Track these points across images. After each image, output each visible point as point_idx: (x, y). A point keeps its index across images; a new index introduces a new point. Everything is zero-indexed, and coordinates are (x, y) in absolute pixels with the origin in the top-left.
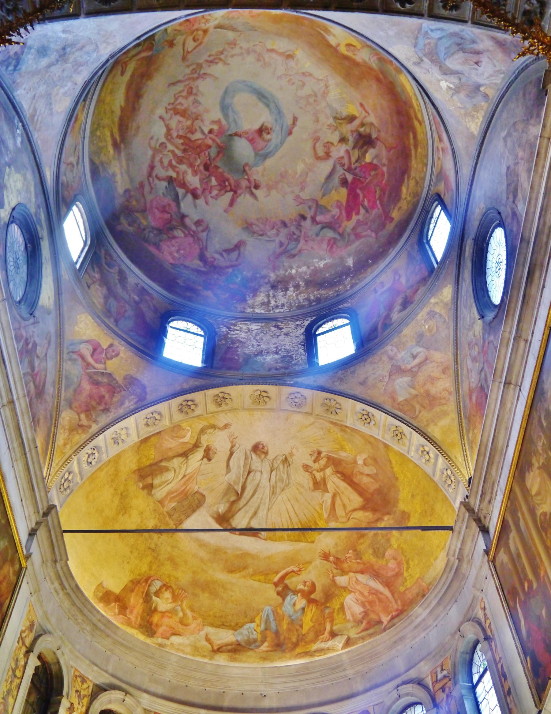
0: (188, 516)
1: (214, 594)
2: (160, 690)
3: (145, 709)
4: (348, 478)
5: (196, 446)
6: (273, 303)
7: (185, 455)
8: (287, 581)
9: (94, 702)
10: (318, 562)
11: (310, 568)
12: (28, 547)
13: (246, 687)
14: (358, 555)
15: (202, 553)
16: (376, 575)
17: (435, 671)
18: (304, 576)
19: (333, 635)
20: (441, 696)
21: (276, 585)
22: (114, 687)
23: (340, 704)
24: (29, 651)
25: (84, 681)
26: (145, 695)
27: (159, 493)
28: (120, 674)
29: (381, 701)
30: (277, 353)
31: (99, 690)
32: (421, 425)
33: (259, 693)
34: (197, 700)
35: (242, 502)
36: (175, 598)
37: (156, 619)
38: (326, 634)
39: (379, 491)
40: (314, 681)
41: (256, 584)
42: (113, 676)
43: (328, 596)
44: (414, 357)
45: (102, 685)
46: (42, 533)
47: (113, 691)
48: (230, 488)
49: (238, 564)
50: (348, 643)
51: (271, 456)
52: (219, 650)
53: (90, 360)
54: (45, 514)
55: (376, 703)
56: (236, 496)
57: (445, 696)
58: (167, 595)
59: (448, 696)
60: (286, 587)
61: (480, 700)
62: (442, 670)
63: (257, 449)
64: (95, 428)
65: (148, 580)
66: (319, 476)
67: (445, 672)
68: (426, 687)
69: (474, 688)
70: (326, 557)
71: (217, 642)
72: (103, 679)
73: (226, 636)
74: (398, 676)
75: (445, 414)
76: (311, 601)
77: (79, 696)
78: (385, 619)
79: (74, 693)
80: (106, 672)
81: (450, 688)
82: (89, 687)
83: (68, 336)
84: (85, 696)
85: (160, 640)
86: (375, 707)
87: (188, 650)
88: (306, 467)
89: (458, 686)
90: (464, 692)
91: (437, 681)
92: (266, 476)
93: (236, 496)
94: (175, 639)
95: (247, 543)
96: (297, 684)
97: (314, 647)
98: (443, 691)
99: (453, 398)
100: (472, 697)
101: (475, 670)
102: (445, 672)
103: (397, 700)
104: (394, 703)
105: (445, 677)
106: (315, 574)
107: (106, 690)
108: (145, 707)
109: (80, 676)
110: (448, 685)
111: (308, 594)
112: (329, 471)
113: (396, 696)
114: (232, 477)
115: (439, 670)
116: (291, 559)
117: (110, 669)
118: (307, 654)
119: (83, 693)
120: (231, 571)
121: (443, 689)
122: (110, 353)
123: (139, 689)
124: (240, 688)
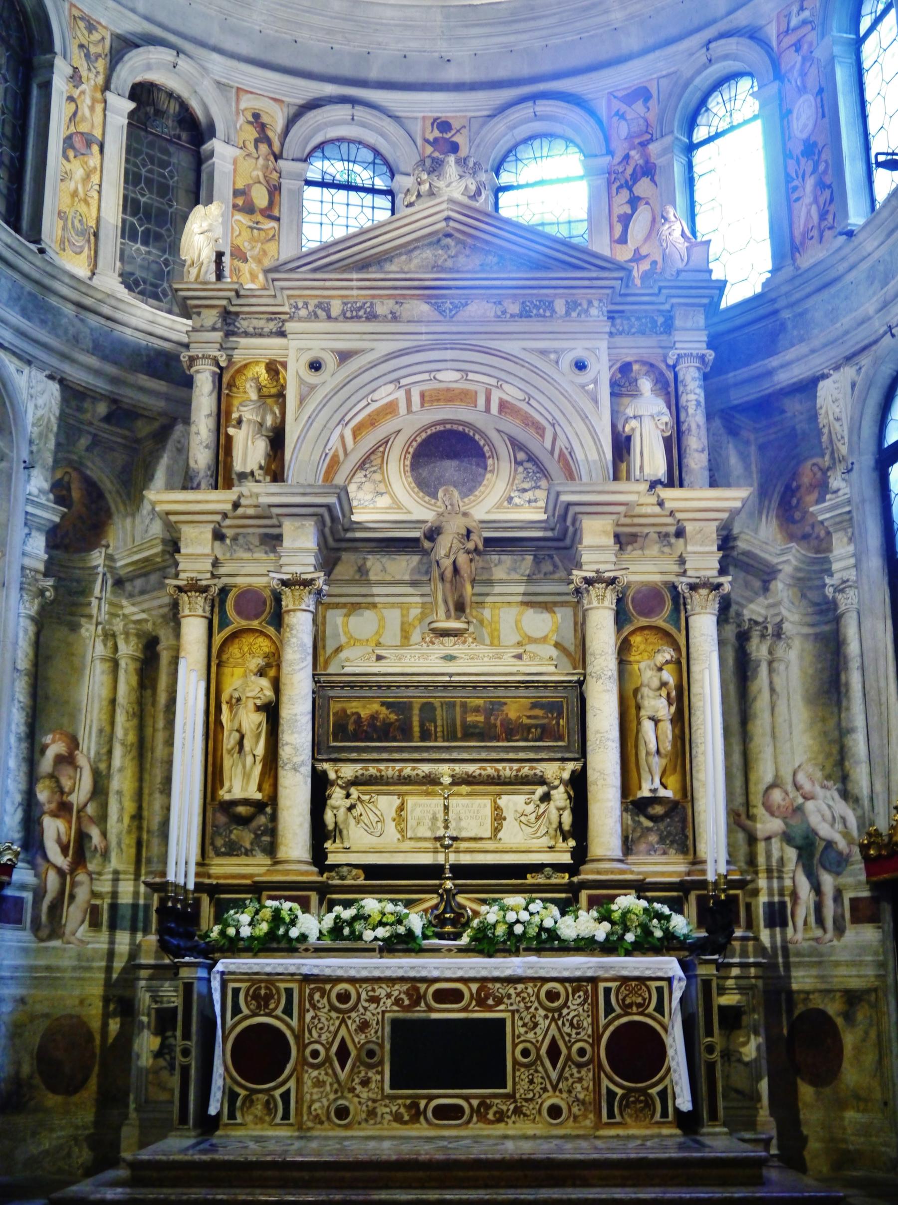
2: (244, 49)
3: (218, 83)
9: (118, 67)
13: (413, 45)
17: (785, 12)
20: (792, 60)
22: (152, 41)
23: (594, 75)
25: (91, 28)
26: (215, 56)
28: (161, 17)
29: (672, 69)
31: (124, 45)
33: (436, 55)
40: (544, 33)
42: (147, 18)
45: (129, 36)
47: (151, 48)
55: (664, 73)
57: (799, 59)
59: (804, 59)
61: (866, 65)
62: (802, 9)
67: (806, 14)
68: (764, 44)
69: (860, 41)
72: (131, 25)
74: (714, 21)
77: (87, 56)
79: (76, 50)
80: (133, 10)
81: (811, 44)
82: (103, 38)
84: (100, 56)
86: (664, 82)
89: (827, 40)
90: (837, 50)
91: (787, 32)
96: (512, 38)
98: (797, 51)
100: (852, 60)
101: (866, 9)
102: (806, 14)
103: (705, 67)
104: (699, 72)
105: (805, 23)
107: (137, 46)
108: (217, 78)
109: (82, 19)
110: (809, 38)
113: (704, 59)
115: (795, 9)
119: (93, 50)
121: (797, 46)
123: (203, 44)
124: (400, 46)
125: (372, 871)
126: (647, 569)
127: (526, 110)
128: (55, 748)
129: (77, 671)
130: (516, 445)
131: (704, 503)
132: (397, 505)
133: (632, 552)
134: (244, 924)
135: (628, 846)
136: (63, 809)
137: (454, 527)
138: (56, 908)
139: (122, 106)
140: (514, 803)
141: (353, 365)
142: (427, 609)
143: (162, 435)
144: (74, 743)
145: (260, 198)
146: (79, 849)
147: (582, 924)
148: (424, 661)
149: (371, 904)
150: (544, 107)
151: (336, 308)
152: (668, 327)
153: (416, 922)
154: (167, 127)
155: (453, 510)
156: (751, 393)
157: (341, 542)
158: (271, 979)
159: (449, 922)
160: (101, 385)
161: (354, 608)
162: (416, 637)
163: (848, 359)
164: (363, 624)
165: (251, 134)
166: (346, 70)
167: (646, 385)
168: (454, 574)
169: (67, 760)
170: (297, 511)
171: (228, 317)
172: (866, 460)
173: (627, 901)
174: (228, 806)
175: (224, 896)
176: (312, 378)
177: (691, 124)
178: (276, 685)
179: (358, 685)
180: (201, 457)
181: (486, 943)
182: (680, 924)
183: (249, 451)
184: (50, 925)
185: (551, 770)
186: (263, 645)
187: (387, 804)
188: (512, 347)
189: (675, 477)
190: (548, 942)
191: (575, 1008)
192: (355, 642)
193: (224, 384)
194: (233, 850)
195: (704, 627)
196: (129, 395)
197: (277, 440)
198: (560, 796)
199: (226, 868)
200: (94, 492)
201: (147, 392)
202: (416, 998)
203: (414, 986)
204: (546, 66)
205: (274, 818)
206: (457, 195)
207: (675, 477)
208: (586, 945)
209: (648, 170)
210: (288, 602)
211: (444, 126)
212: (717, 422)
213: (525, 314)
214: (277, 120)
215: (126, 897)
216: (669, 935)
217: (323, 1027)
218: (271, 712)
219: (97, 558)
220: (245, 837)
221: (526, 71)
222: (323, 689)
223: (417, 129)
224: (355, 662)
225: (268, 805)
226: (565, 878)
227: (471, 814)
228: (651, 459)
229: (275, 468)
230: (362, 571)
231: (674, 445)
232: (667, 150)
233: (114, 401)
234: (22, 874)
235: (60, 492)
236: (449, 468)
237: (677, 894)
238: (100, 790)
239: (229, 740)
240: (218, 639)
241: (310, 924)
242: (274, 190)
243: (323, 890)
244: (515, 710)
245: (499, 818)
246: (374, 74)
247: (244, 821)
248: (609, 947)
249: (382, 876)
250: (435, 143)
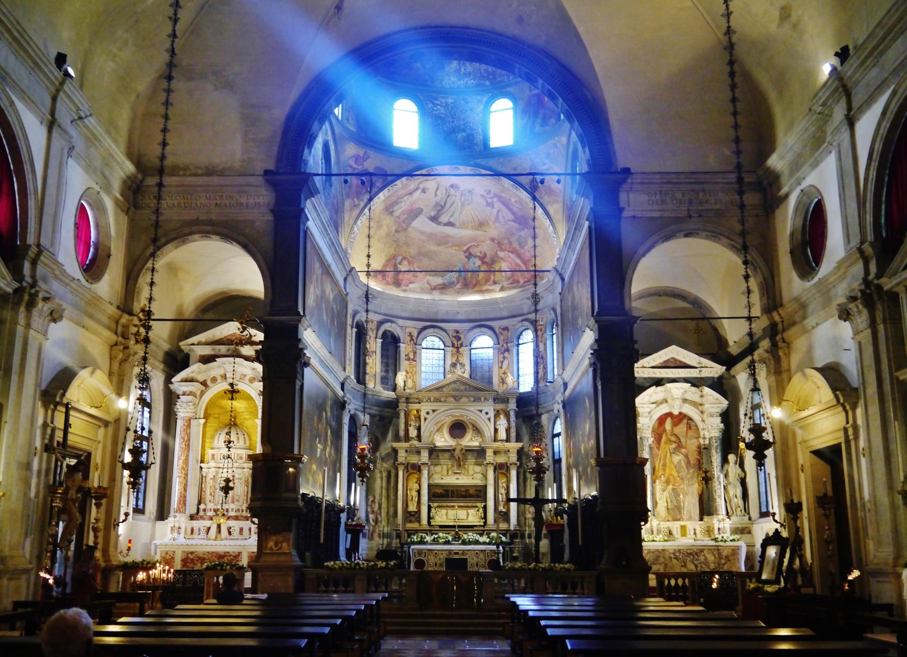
0: (413, 220)
1: (431, 258)
4: (506, 205)
5: (417, 189)
6: (463, 70)
7: (411, 194)
8: (471, 250)
10: (488, 242)
11: (484, 244)
12: (345, 288)
14: (510, 243)
15: (423, 237)
16: (519, 256)
18: (480, 249)
19: (495, 283)
21: (465, 252)
24: (352, 327)
27: (397, 214)
30: (464, 131)
32: (544, 203)
34: (425, 317)
35: (444, 210)
36: (410, 263)
37: (401, 276)
38: (491, 282)
39: (523, 217)
41: (454, 252)
42: (385, 315)
43: (493, 261)
44: (544, 164)
46: (350, 279)
48: (437, 204)
49: (443, 241)
50: (502, 289)
51: (462, 188)
52: (434, 289)
53: (355, 166)
54: (350, 271)
56: (440, 208)
58: (405, 262)
60: (470, 254)
63: (452, 186)
64: (362, 204)
65: (394, 257)
66: (489, 201)
70: (493, 240)
71: (434, 284)
73: (438, 280)
75: (556, 201)
76: (484, 263)
78: (522, 281)
83: (342, 159)
85: (404, 288)
87: (419, 290)
88: (482, 196)
92: (458, 197)
93: (440, 208)
94: (411, 286)
95: (448, 230)
97: (485, 288)
99: (562, 195)
106: (486, 247)
111: (482, 259)
112: (495, 200)
114: (438, 198)
116: (473, 239)
117: (383, 311)
118: (481, 292)
120: (439, 245)
122: (366, 157)
125: (441, 526)
126: (501, 459)
127: (478, 330)
128: (371, 499)
129: (374, 480)
130: (474, 426)
131: (514, 446)
132: (446, 441)
133: (498, 456)
134: (415, 538)
135: (495, 521)
136: (373, 512)
137: (459, 448)
138: (372, 534)
139: (380, 341)
140: (471, 511)
141: (436, 413)
142: (453, 465)
143: (390, 422)
144: (374, 497)
145: (411, 356)
146: (376, 521)
147: (484, 539)
148: (452, 480)
149: (441, 534)
150: (483, 329)
151: (432, 399)
152: (508, 402)
153: (450, 538)
154: (389, 339)
155: (458, 444)
156: (528, 414)
157: (434, 451)
158: (422, 550)
159: (457, 537)
160: (377, 413)
161: (436, 465)
162: (450, 472)
163: (548, 412)
164: (438, 469)
165: (409, 338)
166: (432, 317)
167: (502, 416)
168: (459, 458)
169: (373, 501)
170: (424, 448)
171: (407, 399)
172: (550, 436)
173: (494, 534)
174: (410, 512)
175: (411, 532)
176: (427, 416)
177: (519, 338)
178: (420, 486)
179: (437, 486)
180: (402, 433)
181: (464, 543)
182: (504, 539)
183: (413, 433)
184: (371, 538)
185: (479, 505)
186: (416, 476)
187: (444, 511)
188: (471, 409)
189: (508, 440)
190: (477, 542)
191: (481, 556)
192: (436, 473)
193: (407, 415)
194: (411, 522)
195: (513, 473)
196: (383, 413)
197: (419, 429)
198: (481, 510)
199: (409, 526)
200: (377, 439)
201: (387, 412)
202: (450, 553)
203: (450, 551)
204: (483, 317)
205: (420, 515)
206: (460, 373)
207: (508, 440)
208: (484, 543)
209: (507, 350)
210: (422, 468)
211: (457, 332)
212: (521, 419)
213: (474, 401)
214: (415, 334)
215: (386, 531)
216: (502, 542)
217: (432, 560)
218: (419, 492)
219: (378, 454)
220: (413, 519)
221: (478, 317)
222: (430, 486)
223: (450, 333)
224: (437, 480)
225: (419, 512)
226: (482, 528)
227: (462, 514)
228: (502, 435)
229: (419, 437)
230: (438, 456)
231: (508, 431)
232: (512, 346)
233: (380, 416)
234: (367, 527)
235: (371, 441)
236: (458, 432)
237: (505, 533)
238: (380, 508)
239: (409, 498)
240: (406, 475)
241: (429, 539)
242: (415, 353)
243: (430, 531)
244: (472, 491)
245: (468, 515)
246: (439, 317)
247: (413, 516)
248: (489, 544)
249: (443, 527)
250: (455, 337)
